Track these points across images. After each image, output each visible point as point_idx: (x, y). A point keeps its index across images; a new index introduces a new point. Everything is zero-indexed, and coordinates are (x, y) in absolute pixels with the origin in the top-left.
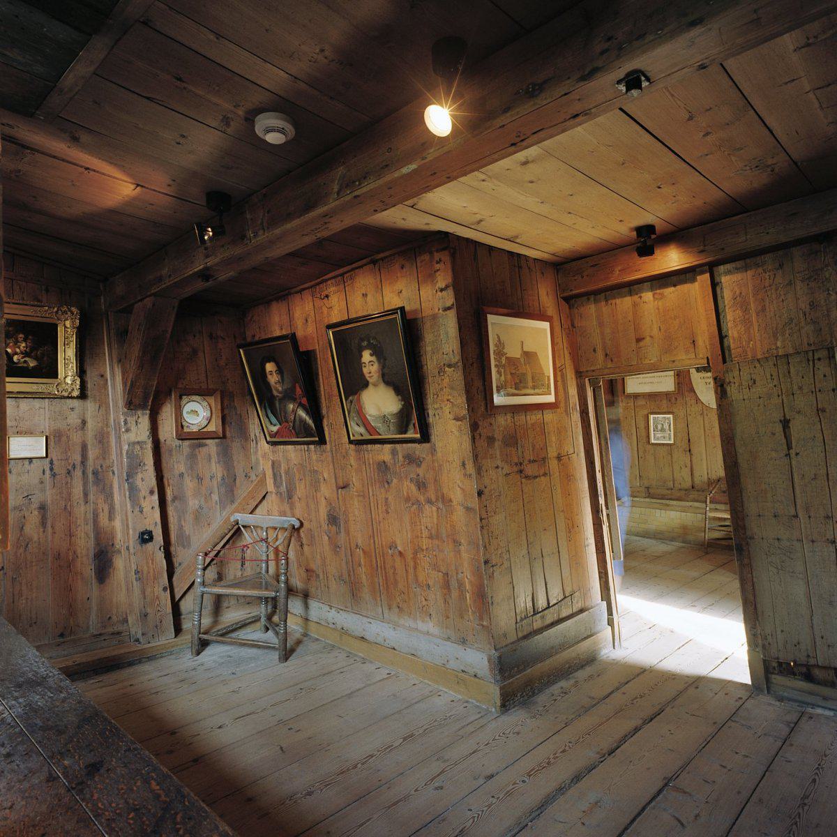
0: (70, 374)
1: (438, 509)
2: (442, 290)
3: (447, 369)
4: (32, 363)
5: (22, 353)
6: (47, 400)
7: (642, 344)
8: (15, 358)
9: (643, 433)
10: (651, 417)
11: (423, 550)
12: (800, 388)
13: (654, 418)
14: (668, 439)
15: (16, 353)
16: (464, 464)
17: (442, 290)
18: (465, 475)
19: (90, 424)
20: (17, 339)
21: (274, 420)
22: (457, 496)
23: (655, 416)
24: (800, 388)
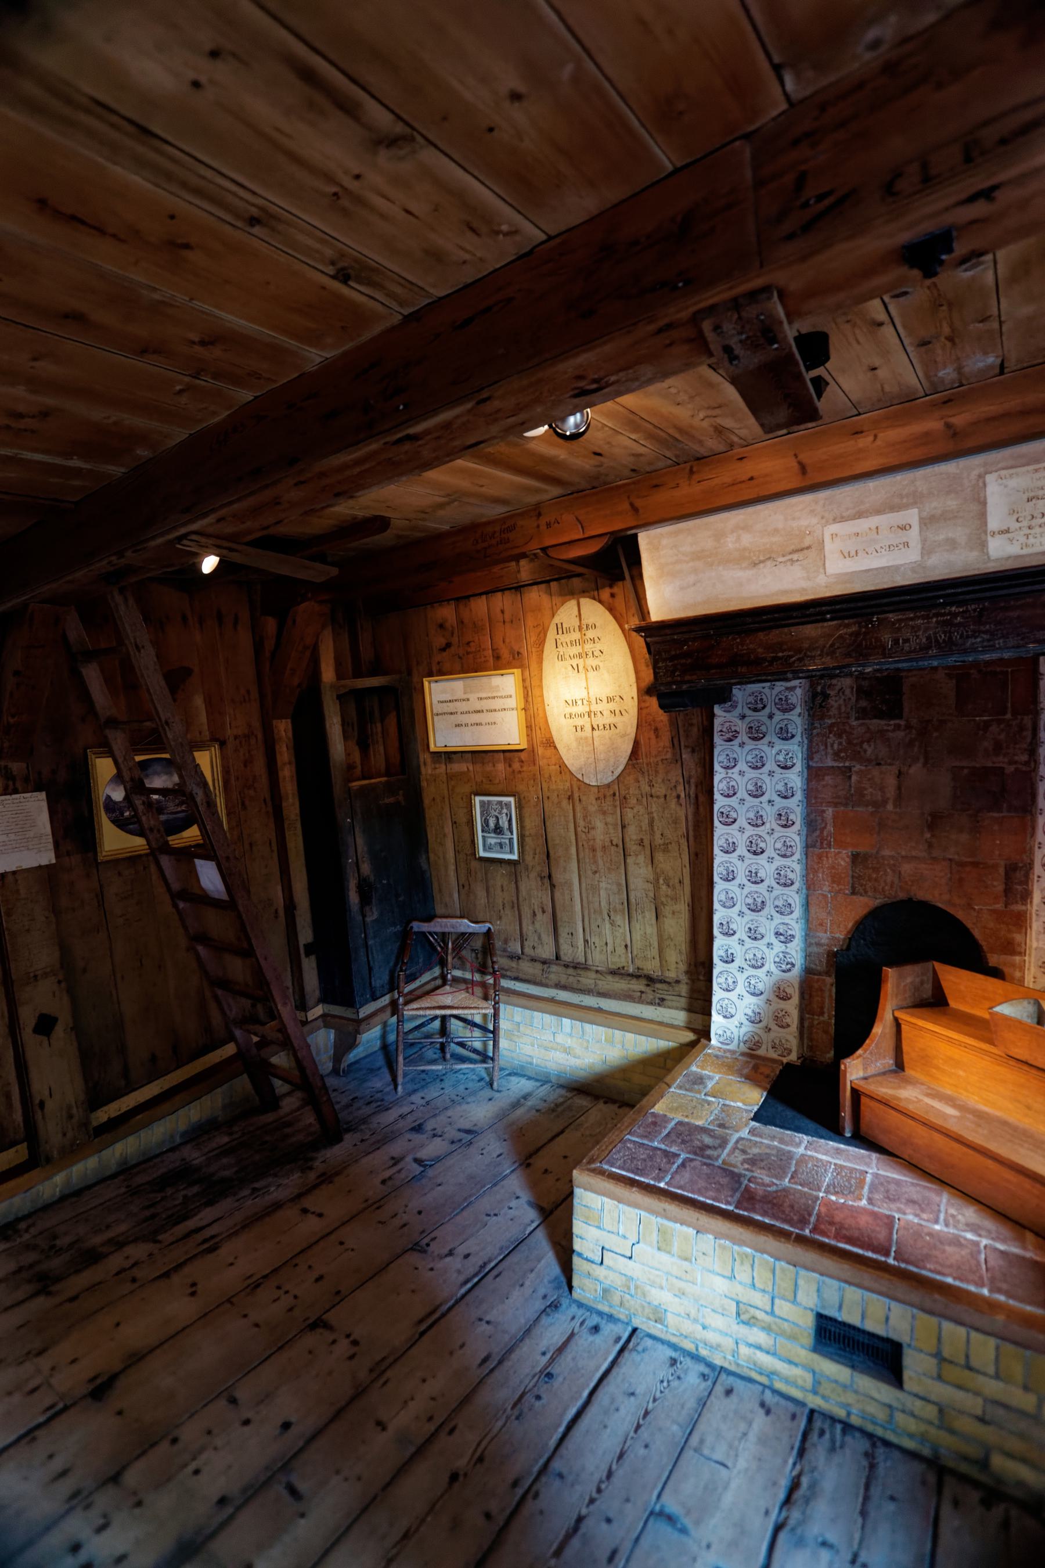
9: (467, 837)
10: (478, 800)
13: (482, 803)
14: (508, 849)
23: (486, 799)
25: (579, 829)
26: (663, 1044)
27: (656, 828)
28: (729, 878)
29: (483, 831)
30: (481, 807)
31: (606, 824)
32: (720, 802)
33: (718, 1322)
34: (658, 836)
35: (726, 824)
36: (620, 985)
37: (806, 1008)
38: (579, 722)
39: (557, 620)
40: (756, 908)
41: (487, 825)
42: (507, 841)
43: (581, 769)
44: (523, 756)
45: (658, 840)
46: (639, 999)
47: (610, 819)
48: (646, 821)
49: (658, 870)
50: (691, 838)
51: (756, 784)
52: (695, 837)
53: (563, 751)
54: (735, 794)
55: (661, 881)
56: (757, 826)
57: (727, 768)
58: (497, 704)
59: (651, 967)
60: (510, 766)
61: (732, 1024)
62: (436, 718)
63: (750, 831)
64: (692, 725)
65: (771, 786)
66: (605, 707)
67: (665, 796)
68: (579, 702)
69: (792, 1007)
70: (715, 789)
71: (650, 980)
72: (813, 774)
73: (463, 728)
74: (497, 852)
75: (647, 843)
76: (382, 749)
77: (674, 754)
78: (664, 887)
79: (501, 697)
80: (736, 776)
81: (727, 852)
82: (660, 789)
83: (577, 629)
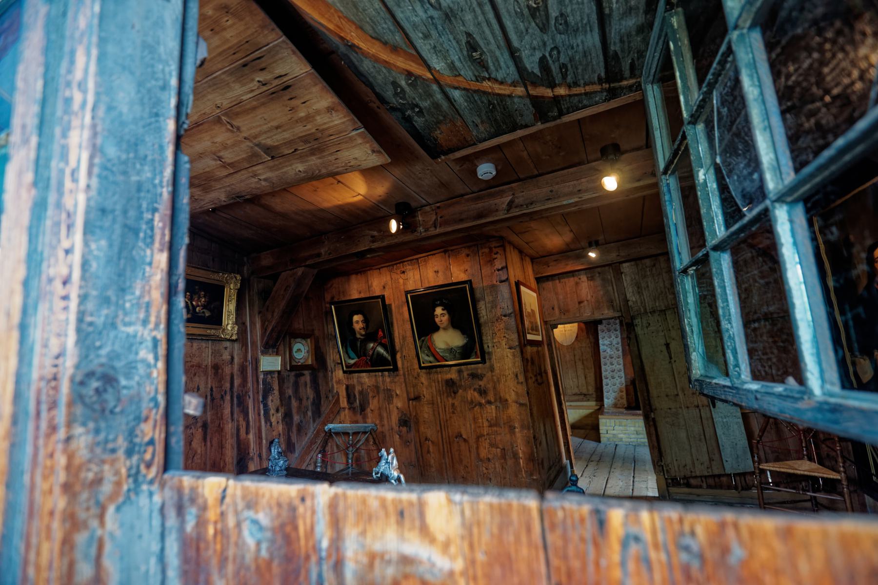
0: (230, 322)
1: (496, 407)
2: (498, 270)
3: (503, 318)
4: (207, 314)
5: (202, 306)
6: (210, 342)
7: (582, 305)
8: (198, 309)
11: (484, 436)
12: (673, 327)
15: (198, 306)
16: (517, 376)
17: (498, 270)
18: (518, 383)
19: (236, 360)
20: (199, 295)
21: (352, 354)
22: (511, 396)
24: (673, 327)
26: (591, 411)
28: (605, 364)
33: (633, 436)
36: (576, 398)
37: (627, 394)
40: (613, 371)
45: (584, 358)
46: (582, 401)
59: (584, 391)
61: (610, 401)
65: (614, 342)
69: (624, 394)
71: (585, 395)
72: (622, 339)
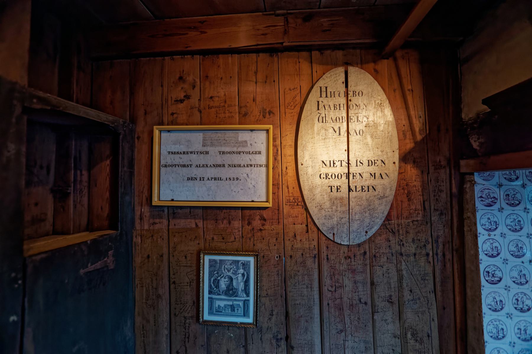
9: (189, 298)
10: (207, 258)
13: (212, 263)
14: (241, 311)
23: (218, 258)
25: (325, 289)
27: (405, 285)
29: (210, 292)
30: (210, 266)
31: (355, 282)
32: (485, 262)
34: (406, 293)
35: (493, 283)
38: (336, 183)
39: (321, 83)
41: (217, 286)
42: (241, 304)
43: (333, 228)
44: (265, 214)
47: (359, 278)
48: (396, 279)
49: (406, 325)
50: (439, 294)
51: (517, 245)
52: (443, 291)
53: (313, 211)
54: (498, 254)
55: (409, 336)
56: (521, 284)
57: (490, 230)
58: (245, 159)
60: (249, 224)
62: (163, 170)
63: (515, 289)
64: (441, 191)
66: (365, 170)
67: (415, 255)
68: (338, 164)
70: (480, 250)
73: (197, 182)
74: (227, 315)
75: (395, 299)
76: (85, 200)
77: (424, 216)
78: (412, 342)
79: (249, 153)
80: (498, 237)
81: (495, 310)
82: (411, 248)
83: (342, 94)
